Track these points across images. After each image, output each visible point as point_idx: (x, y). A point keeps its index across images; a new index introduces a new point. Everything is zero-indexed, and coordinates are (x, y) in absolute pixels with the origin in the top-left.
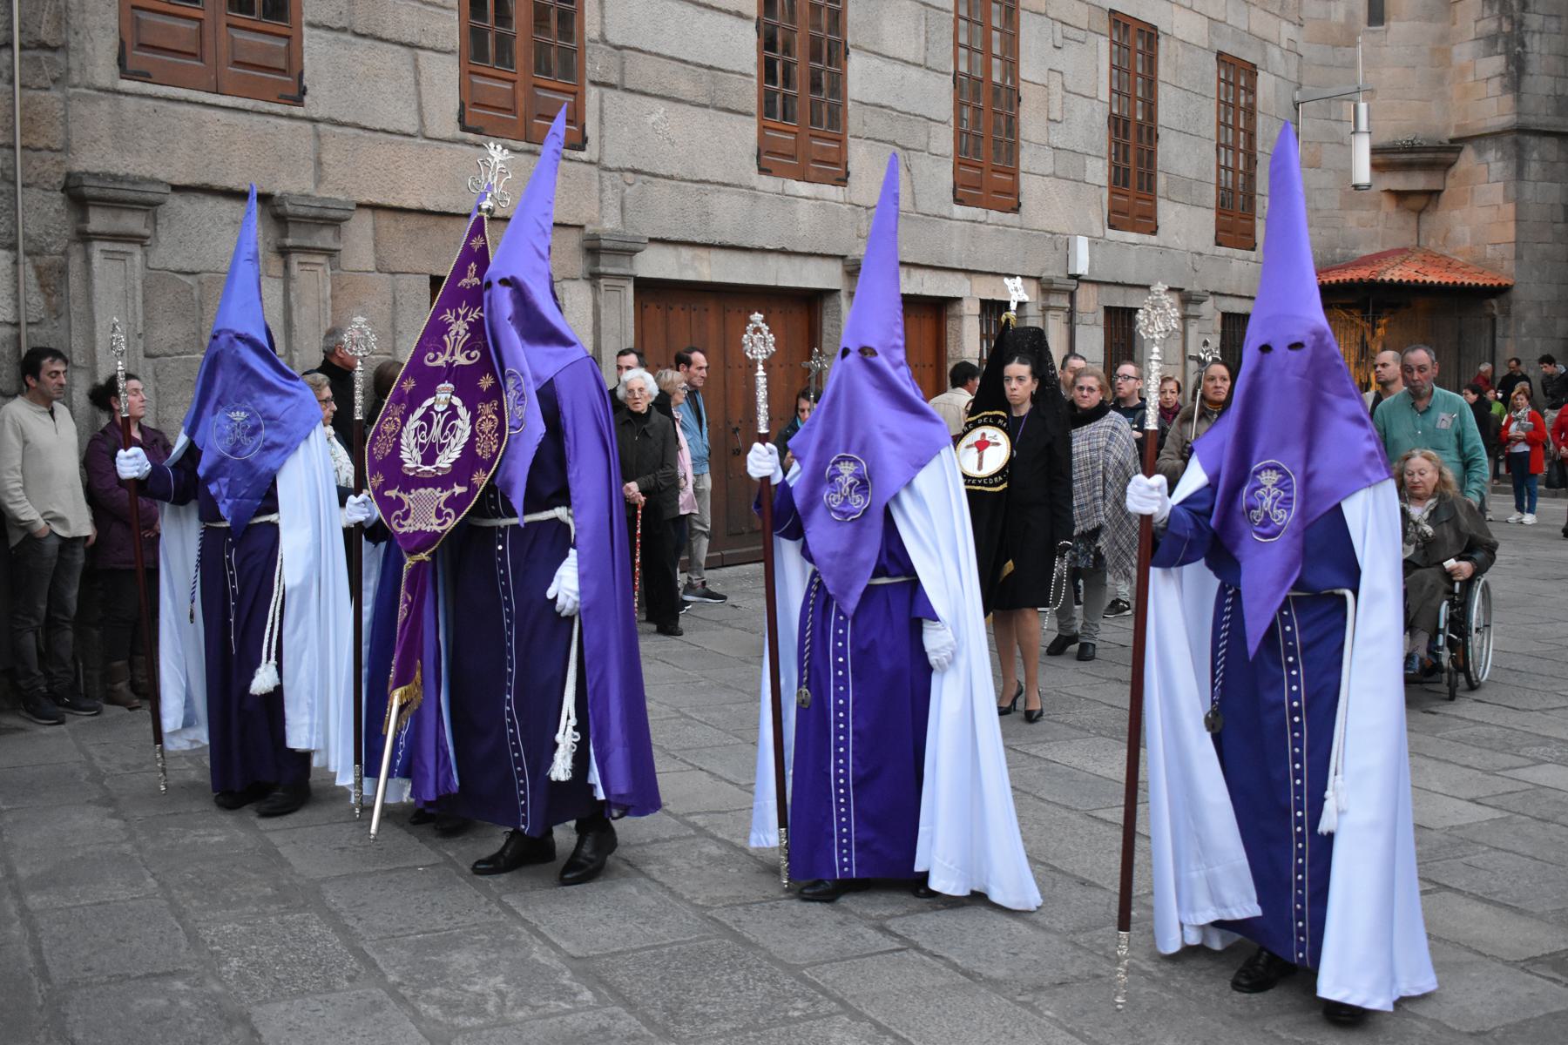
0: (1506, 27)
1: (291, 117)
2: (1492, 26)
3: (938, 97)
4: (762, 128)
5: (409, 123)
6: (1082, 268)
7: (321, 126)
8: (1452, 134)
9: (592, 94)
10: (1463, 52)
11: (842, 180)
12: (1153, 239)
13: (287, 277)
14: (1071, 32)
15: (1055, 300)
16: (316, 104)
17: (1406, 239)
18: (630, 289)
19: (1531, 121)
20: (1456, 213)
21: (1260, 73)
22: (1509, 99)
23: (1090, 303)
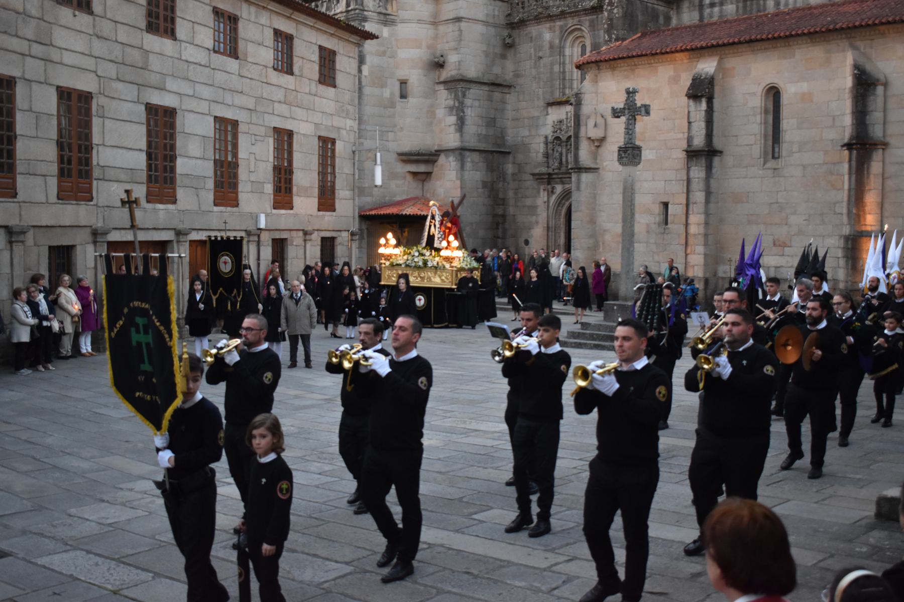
0: (457, 104)
1: (14, 202)
2: (451, 103)
3: (207, 169)
4: (148, 188)
5: (44, 200)
6: (262, 225)
7: (21, 204)
8: (436, 148)
9: (95, 183)
10: (441, 112)
11: (174, 202)
12: (291, 212)
13: (11, 250)
14: (257, 138)
15: (252, 238)
16: (20, 197)
17: (418, 193)
18: (106, 244)
19: (467, 145)
20: (438, 182)
21: (337, 141)
22: (458, 135)
23: (266, 238)
